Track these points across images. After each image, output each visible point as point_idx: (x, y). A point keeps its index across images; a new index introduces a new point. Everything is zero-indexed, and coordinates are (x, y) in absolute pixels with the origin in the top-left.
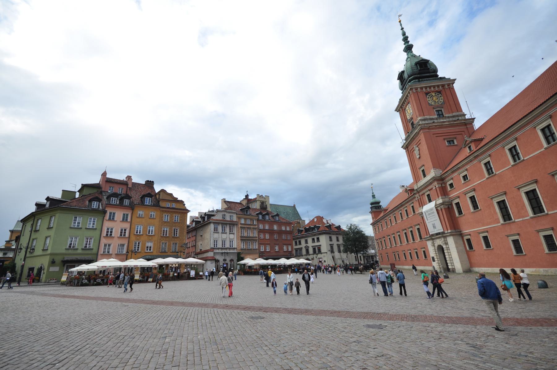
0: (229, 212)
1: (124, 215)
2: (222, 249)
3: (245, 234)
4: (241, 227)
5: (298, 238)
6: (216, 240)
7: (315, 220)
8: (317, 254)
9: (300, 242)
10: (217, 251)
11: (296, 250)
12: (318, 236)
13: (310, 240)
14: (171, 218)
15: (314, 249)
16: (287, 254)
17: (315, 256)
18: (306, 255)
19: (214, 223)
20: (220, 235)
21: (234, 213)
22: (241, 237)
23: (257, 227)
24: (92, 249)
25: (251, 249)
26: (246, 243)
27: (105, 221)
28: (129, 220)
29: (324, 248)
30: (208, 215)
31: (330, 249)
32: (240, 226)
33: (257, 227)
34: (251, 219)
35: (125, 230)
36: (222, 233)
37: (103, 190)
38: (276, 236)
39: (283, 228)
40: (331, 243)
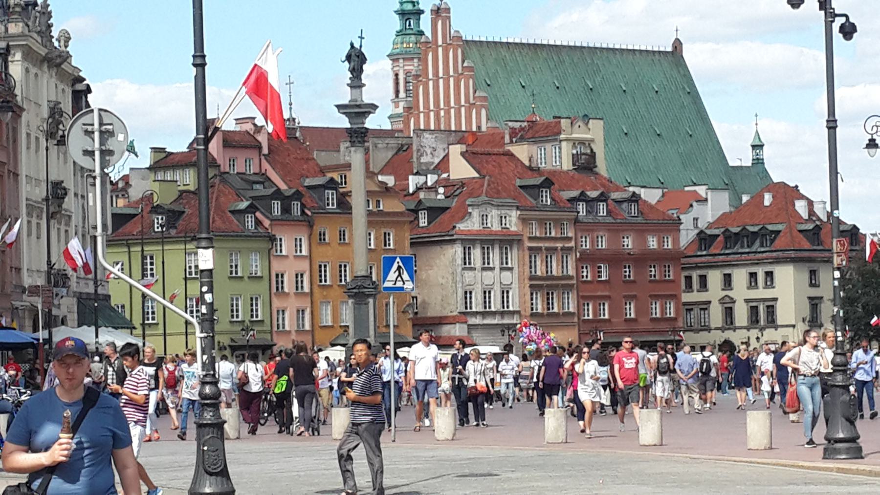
0: (498, 206)
1: (296, 239)
2: (484, 314)
3: (540, 271)
4: (530, 249)
5: (697, 267)
6: (468, 288)
7: (768, 199)
8: (762, 329)
9: (703, 279)
10: (473, 321)
11: (689, 307)
12: (769, 268)
13: (740, 276)
14: (376, 238)
15: (754, 311)
16: (663, 326)
17: (754, 333)
18: (722, 329)
19: (463, 241)
20: (478, 274)
21: (509, 206)
22: (531, 278)
23: (572, 244)
24: (262, 321)
25: (556, 315)
26: (542, 296)
27: (272, 258)
28: (305, 252)
29: (786, 312)
30: (430, 209)
31: (807, 312)
32: (528, 244)
33: (572, 244)
34: (559, 223)
35: (302, 275)
36: (483, 269)
37: (222, 170)
38: (629, 273)
39: (653, 243)
40: (814, 292)
